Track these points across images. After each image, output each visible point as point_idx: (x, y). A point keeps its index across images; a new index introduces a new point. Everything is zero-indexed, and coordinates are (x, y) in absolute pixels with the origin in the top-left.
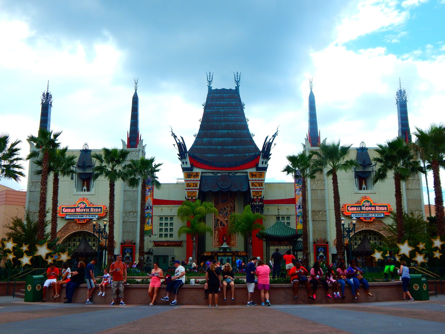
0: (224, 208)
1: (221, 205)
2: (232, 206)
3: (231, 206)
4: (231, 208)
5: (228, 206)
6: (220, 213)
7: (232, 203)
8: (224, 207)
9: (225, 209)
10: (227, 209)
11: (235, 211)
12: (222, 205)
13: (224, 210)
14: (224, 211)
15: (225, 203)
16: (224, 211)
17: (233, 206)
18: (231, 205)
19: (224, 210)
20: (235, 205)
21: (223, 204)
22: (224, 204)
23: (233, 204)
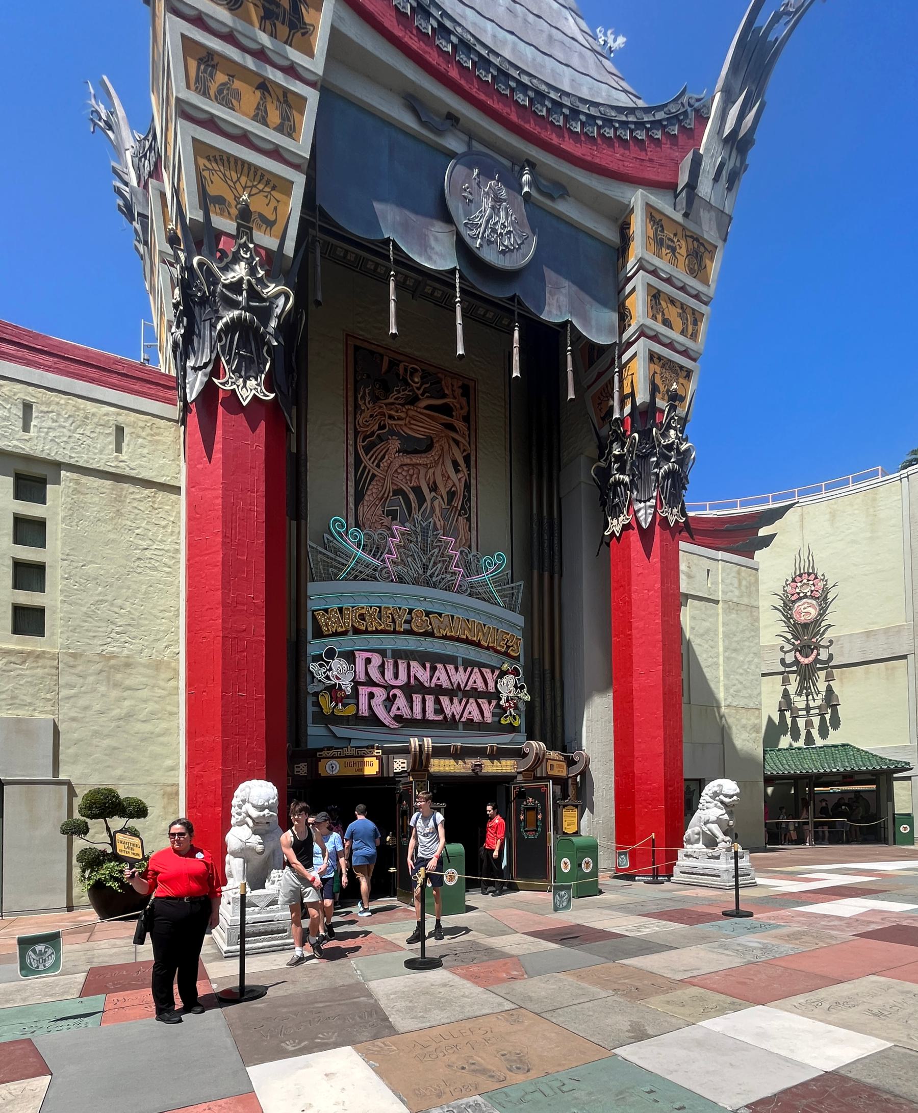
0: (413, 488)
1: (397, 463)
2: (454, 485)
3: (450, 484)
4: (452, 495)
5: (435, 482)
6: (393, 515)
7: (455, 464)
8: (413, 484)
9: (421, 500)
10: (428, 496)
11: (469, 519)
12: (406, 465)
13: (412, 496)
14: (414, 505)
15: (416, 459)
16: (414, 505)
17: (460, 487)
18: (449, 477)
19: (412, 496)
20: (467, 487)
21: (407, 461)
22: (414, 465)
23: (460, 476)
